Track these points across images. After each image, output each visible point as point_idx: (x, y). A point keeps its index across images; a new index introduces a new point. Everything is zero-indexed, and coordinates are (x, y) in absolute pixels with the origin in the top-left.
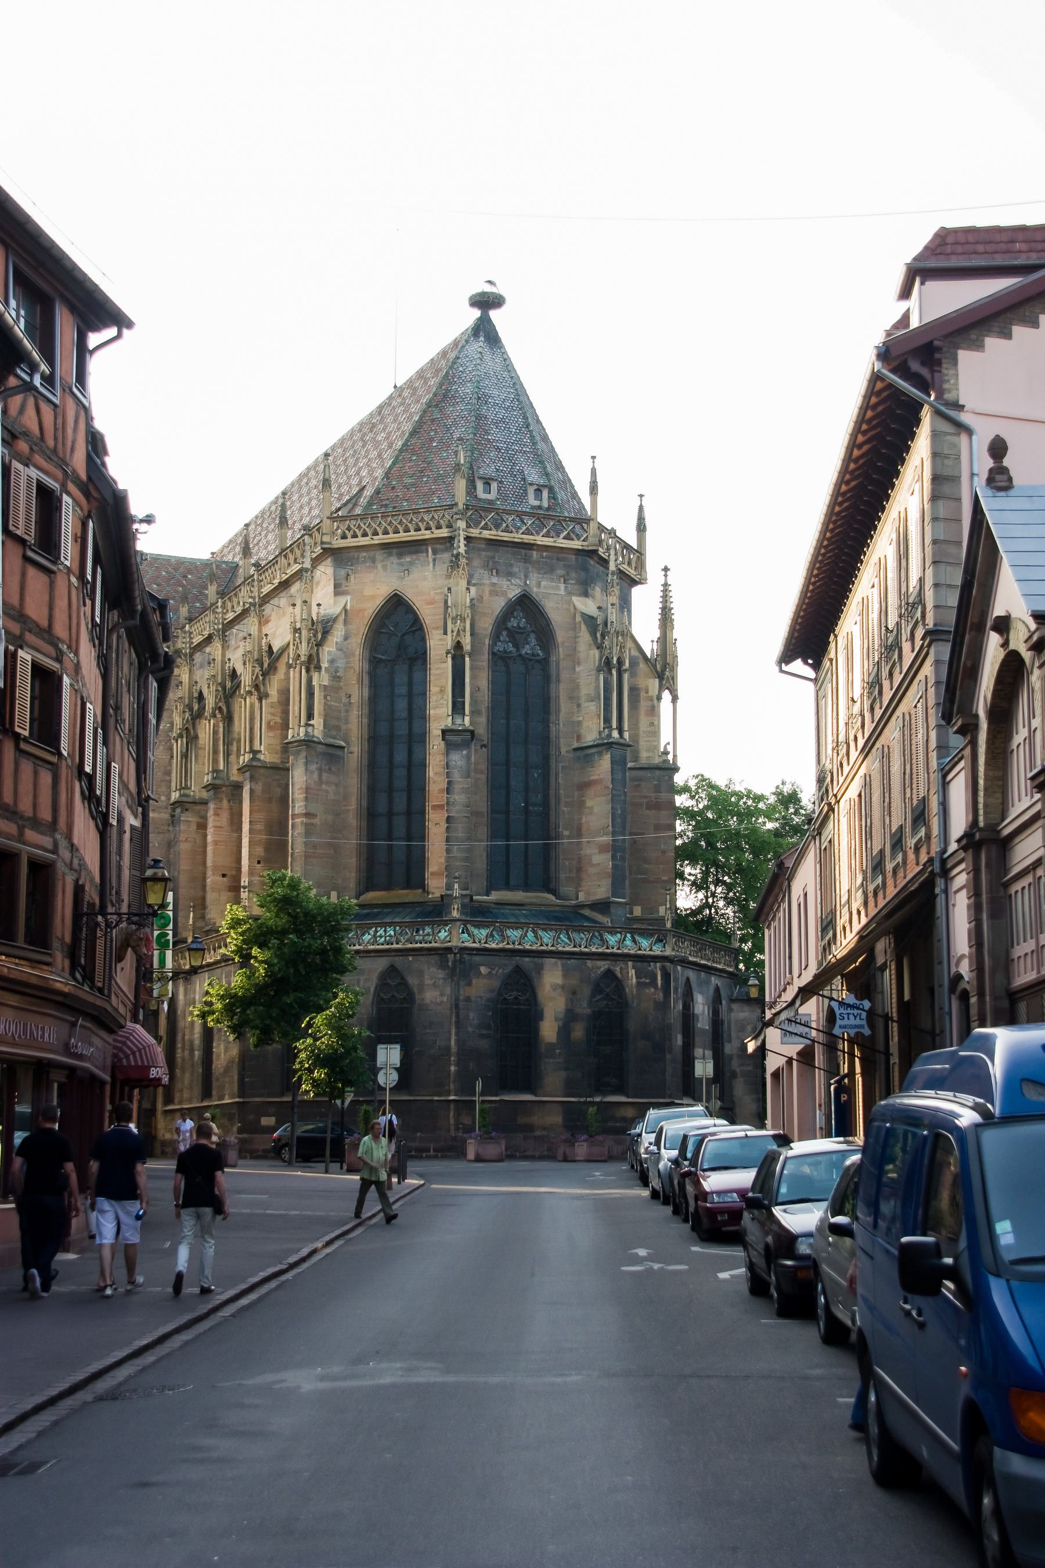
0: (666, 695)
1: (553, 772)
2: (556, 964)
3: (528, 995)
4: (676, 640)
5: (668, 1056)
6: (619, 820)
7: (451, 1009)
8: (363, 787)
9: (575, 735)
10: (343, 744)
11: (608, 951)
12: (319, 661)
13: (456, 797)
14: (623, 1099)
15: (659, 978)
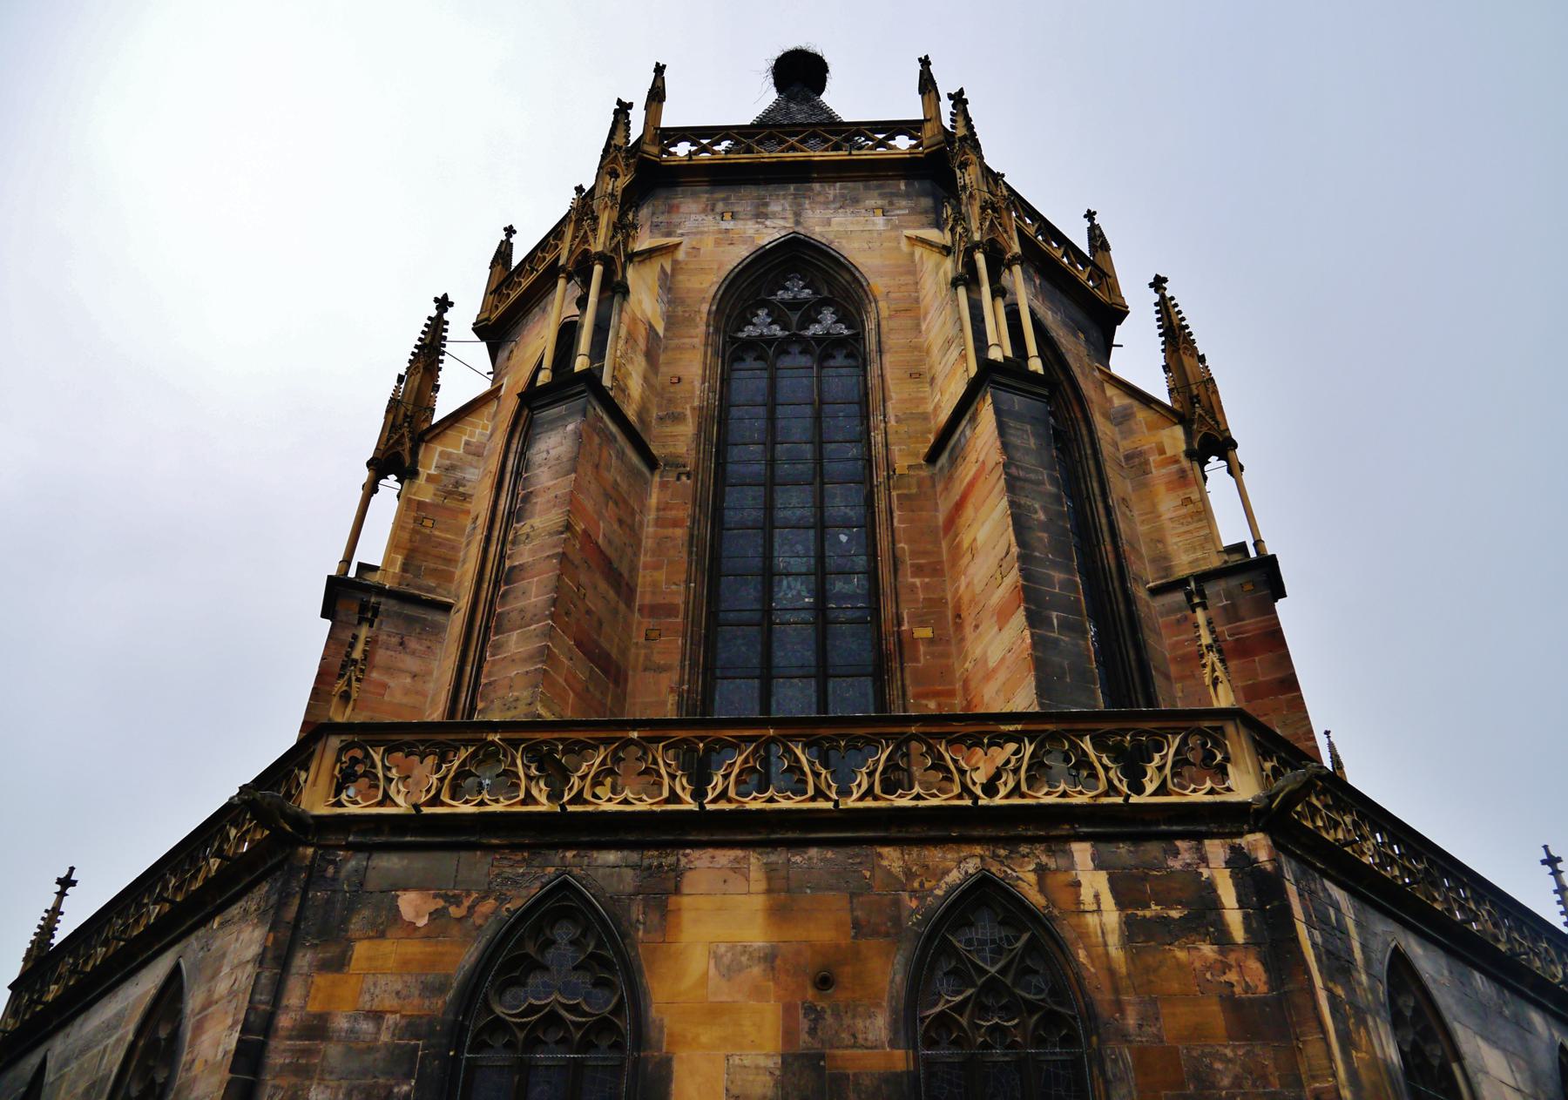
0: (1215, 467)
2: (737, 869)
12: (415, 462)
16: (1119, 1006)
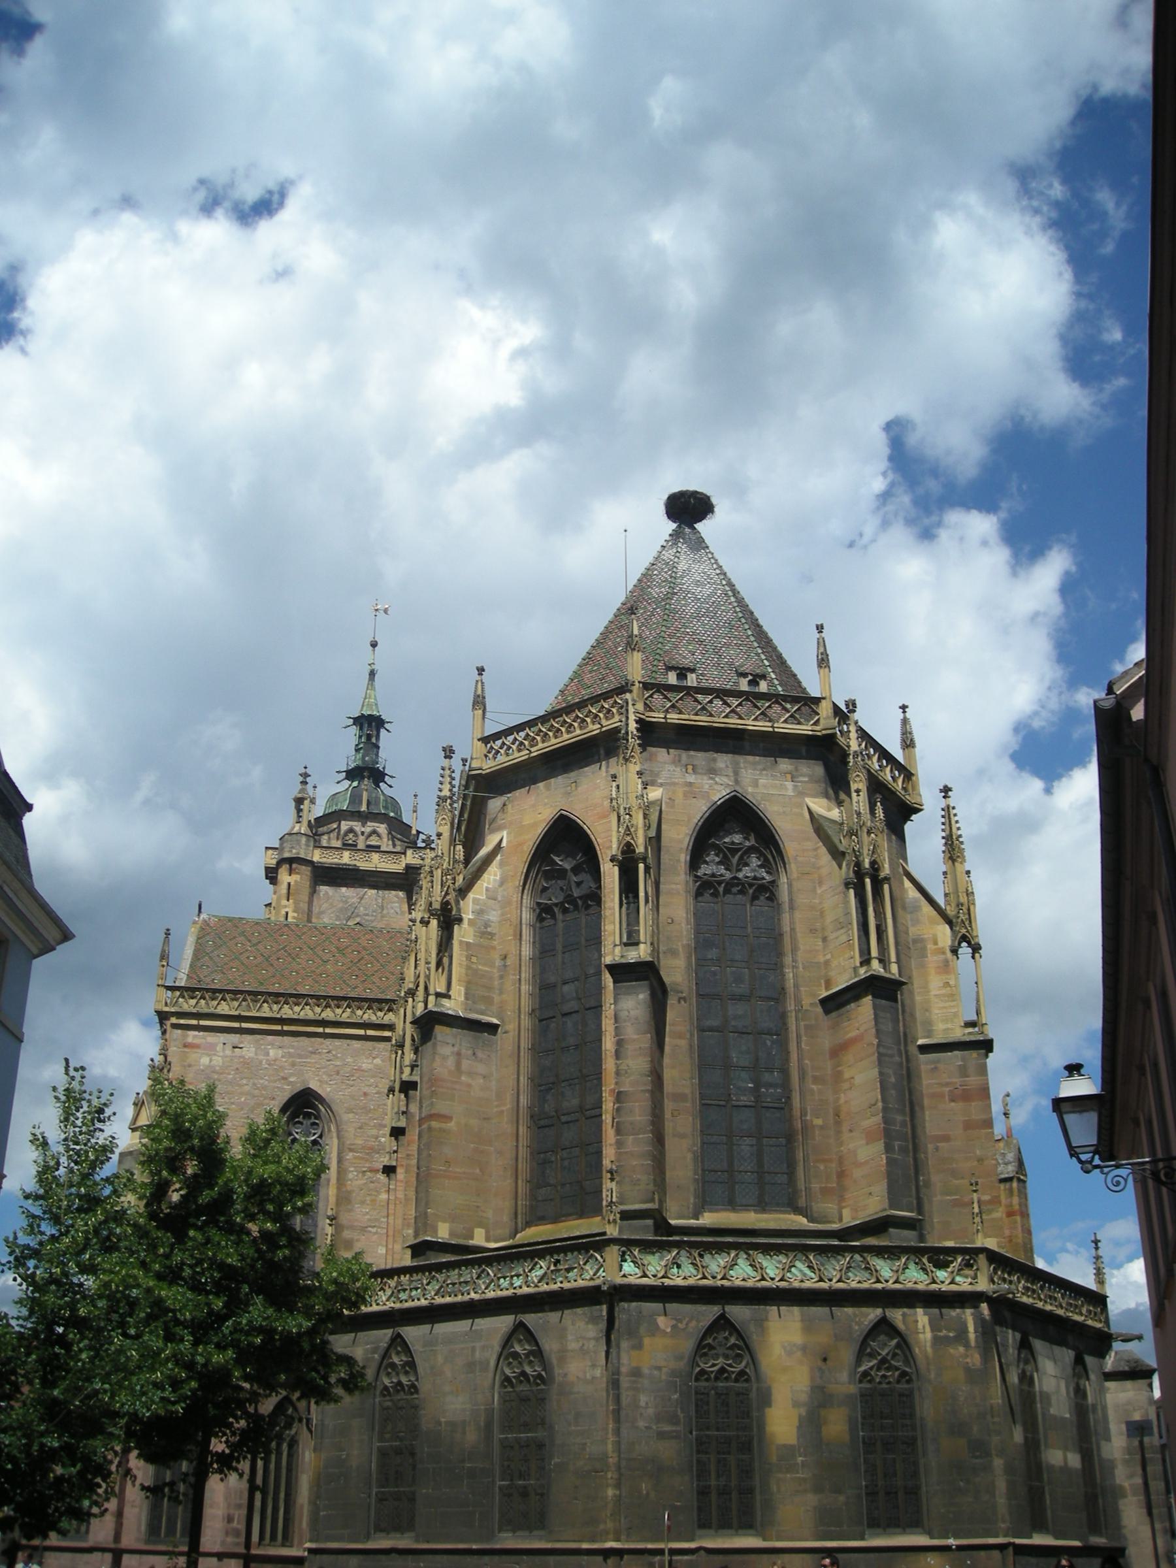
1: (793, 1036)
3: (744, 1364)
4: (968, 872)
5: (998, 1463)
6: (893, 1092)
7: (607, 1390)
8: (521, 1078)
9: (823, 982)
10: (495, 1021)
11: (879, 1286)
13: (630, 1062)
14: (922, 1540)
15: (971, 1328)
16: (929, 1370)
